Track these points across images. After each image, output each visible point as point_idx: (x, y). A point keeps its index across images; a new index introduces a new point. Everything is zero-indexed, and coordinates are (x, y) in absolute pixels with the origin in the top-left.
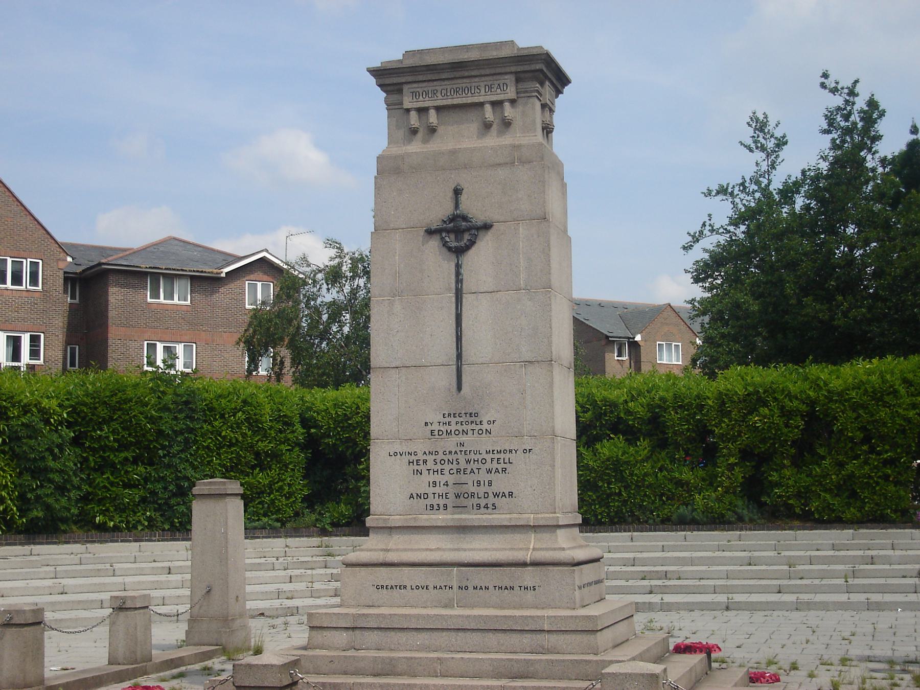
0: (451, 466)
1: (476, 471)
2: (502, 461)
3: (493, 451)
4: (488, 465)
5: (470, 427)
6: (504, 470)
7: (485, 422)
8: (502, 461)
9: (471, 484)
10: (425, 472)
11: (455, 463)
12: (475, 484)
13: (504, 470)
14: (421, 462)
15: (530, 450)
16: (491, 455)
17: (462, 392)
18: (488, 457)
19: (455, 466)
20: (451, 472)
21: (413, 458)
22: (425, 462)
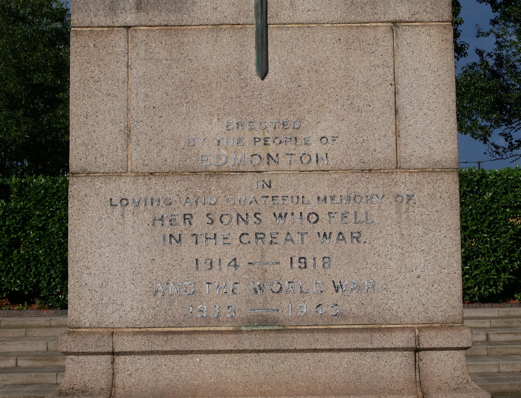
0: (242, 227)
1: (297, 238)
2: (351, 217)
3: (333, 198)
4: (323, 227)
5: (282, 149)
6: (356, 237)
7: (314, 139)
8: (351, 217)
9: (285, 262)
10: (188, 241)
11: (252, 220)
12: (296, 265)
13: (356, 237)
14: (180, 219)
15: (410, 198)
16: (329, 206)
17: (266, 80)
18: (322, 210)
19: (252, 227)
20: (245, 239)
21: (162, 211)
22: (187, 218)
